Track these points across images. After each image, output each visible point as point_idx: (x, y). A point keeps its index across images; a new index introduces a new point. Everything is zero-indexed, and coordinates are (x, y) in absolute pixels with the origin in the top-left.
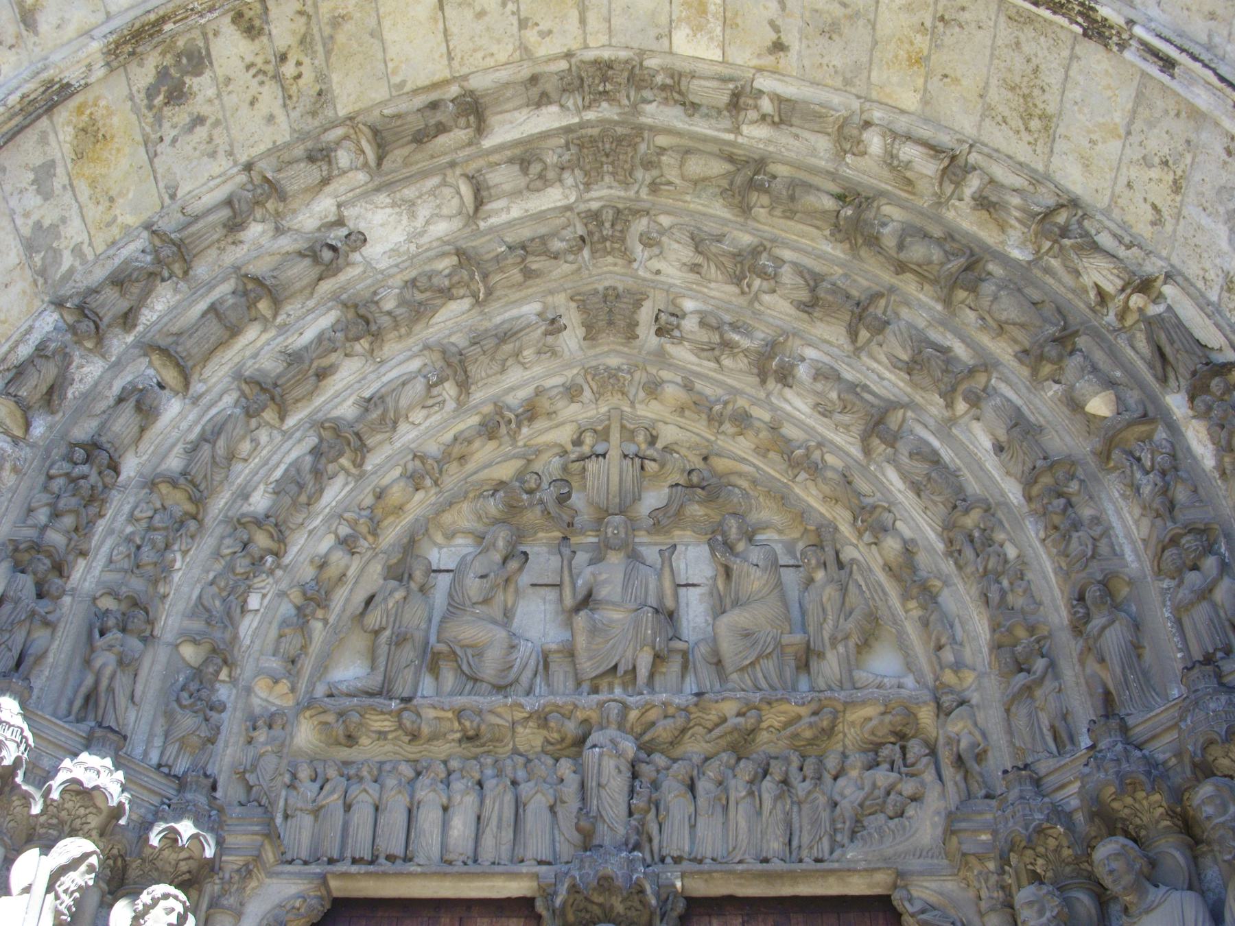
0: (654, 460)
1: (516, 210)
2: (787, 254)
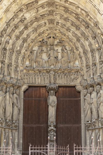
0: (56, 38)
1: (41, 11)
2: (70, 19)
